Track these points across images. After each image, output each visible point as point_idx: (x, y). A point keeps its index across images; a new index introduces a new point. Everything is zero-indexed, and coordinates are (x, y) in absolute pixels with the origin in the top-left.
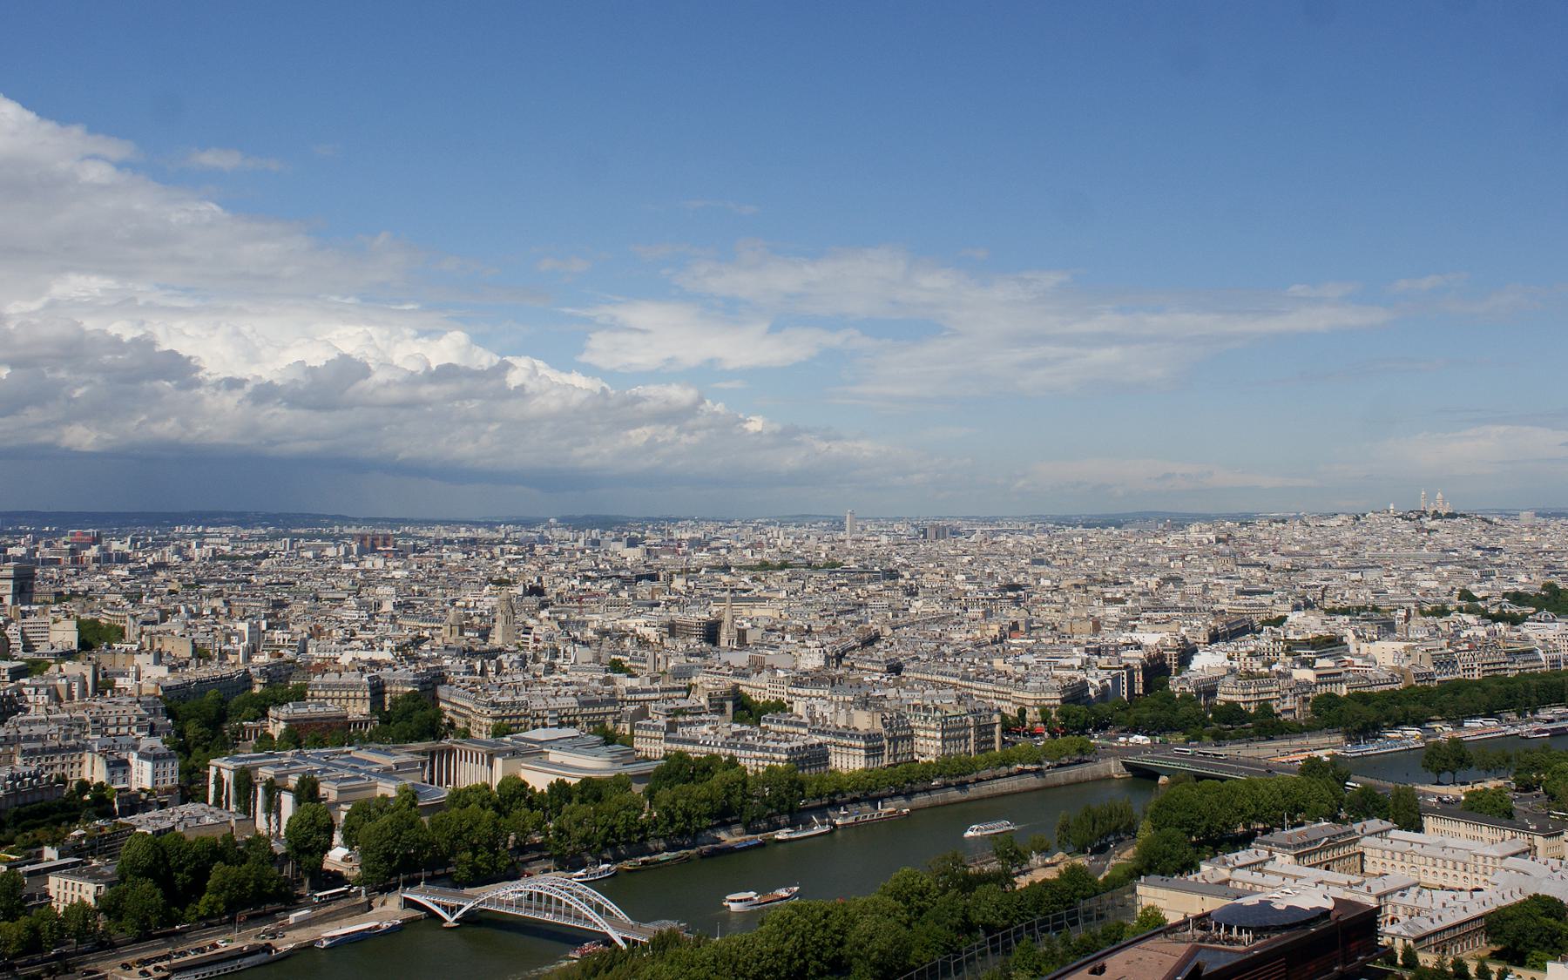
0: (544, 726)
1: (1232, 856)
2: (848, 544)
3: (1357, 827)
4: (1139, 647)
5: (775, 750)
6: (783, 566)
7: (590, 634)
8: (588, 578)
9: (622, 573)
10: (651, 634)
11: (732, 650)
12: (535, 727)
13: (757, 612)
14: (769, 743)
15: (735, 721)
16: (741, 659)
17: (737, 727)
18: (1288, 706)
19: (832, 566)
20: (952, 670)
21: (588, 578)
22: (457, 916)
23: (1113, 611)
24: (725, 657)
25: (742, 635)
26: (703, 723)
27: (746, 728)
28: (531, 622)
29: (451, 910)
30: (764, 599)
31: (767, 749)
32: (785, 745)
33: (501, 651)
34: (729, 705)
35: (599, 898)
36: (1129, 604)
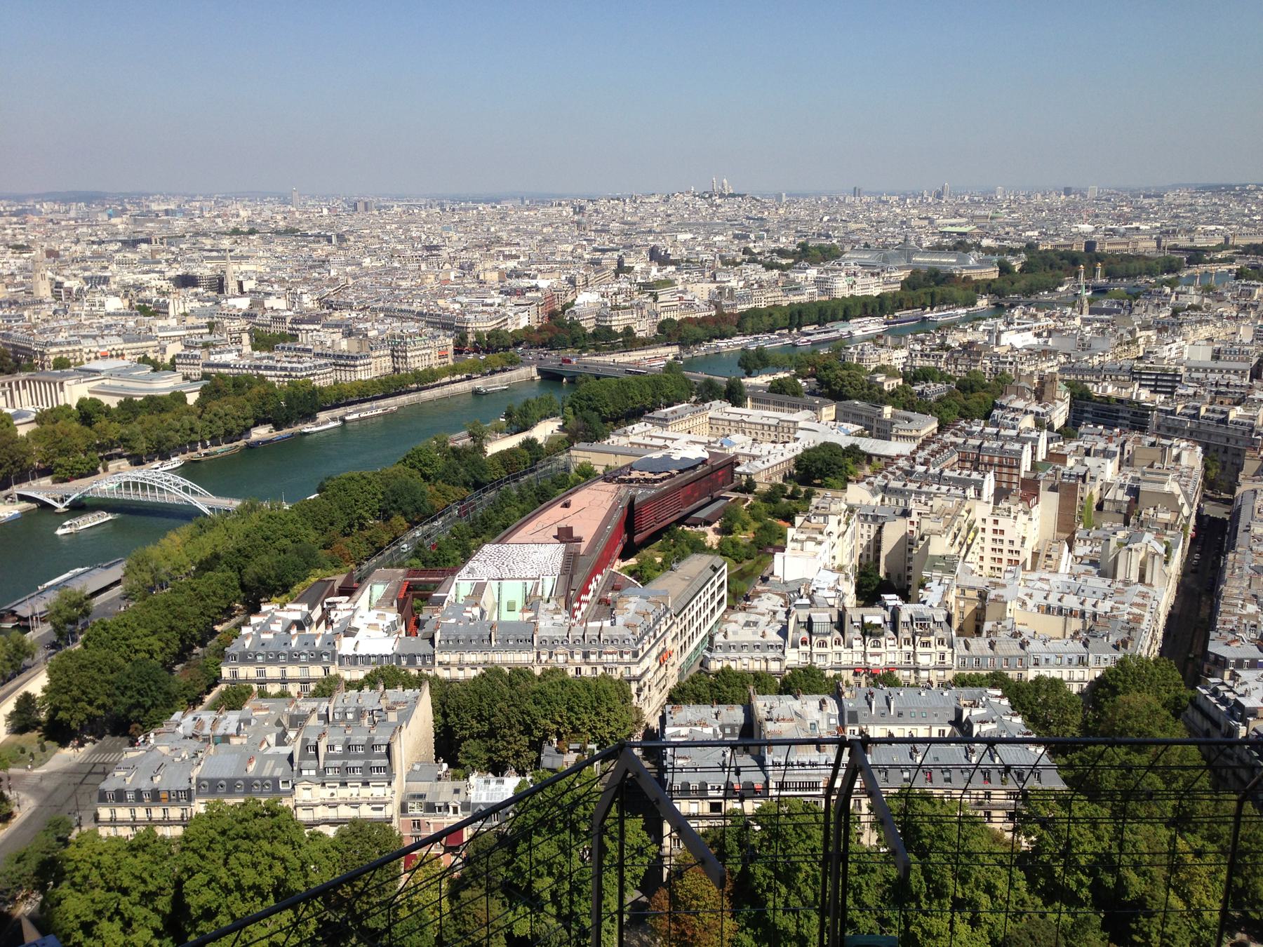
0: (96, 358)
1: (630, 428)
2: (297, 215)
3: (707, 405)
4: (537, 289)
5: (292, 369)
6: (252, 232)
7: (114, 287)
8: (93, 243)
9: (121, 238)
10: (165, 285)
11: (235, 297)
12: (89, 360)
13: (244, 267)
14: (287, 365)
15: (255, 348)
16: (243, 303)
17: (257, 354)
18: (643, 328)
19: (290, 232)
20: (405, 307)
21: (93, 243)
22: (67, 503)
23: (512, 264)
24: (231, 302)
25: (240, 284)
26: (230, 351)
27: (265, 354)
28: (59, 279)
29: (62, 501)
30: (248, 257)
31: (285, 369)
32: (300, 366)
33: (41, 302)
34: (246, 337)
35: (188, 483)
36: (522, 259)
